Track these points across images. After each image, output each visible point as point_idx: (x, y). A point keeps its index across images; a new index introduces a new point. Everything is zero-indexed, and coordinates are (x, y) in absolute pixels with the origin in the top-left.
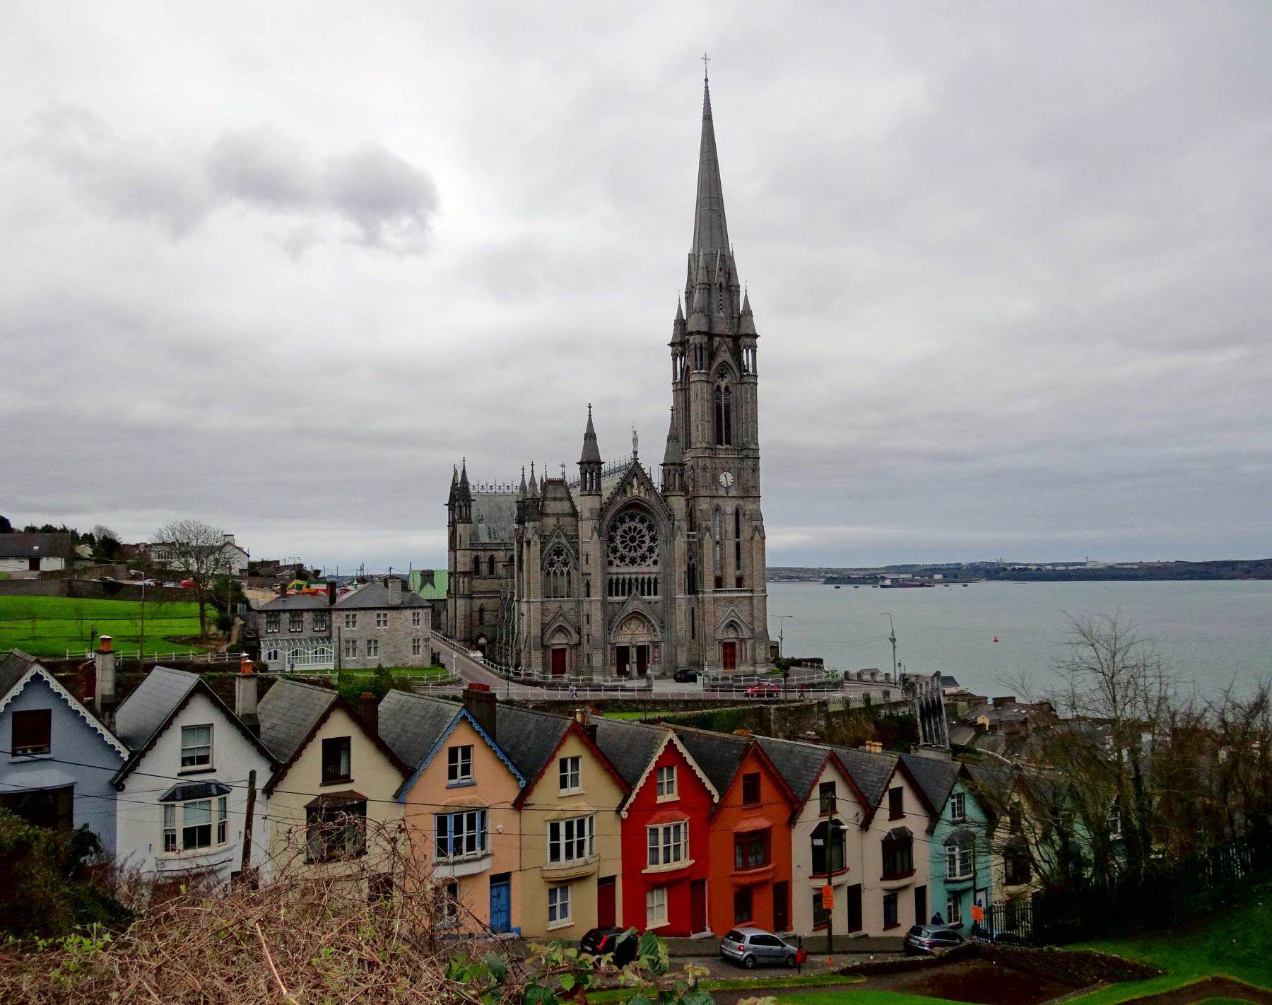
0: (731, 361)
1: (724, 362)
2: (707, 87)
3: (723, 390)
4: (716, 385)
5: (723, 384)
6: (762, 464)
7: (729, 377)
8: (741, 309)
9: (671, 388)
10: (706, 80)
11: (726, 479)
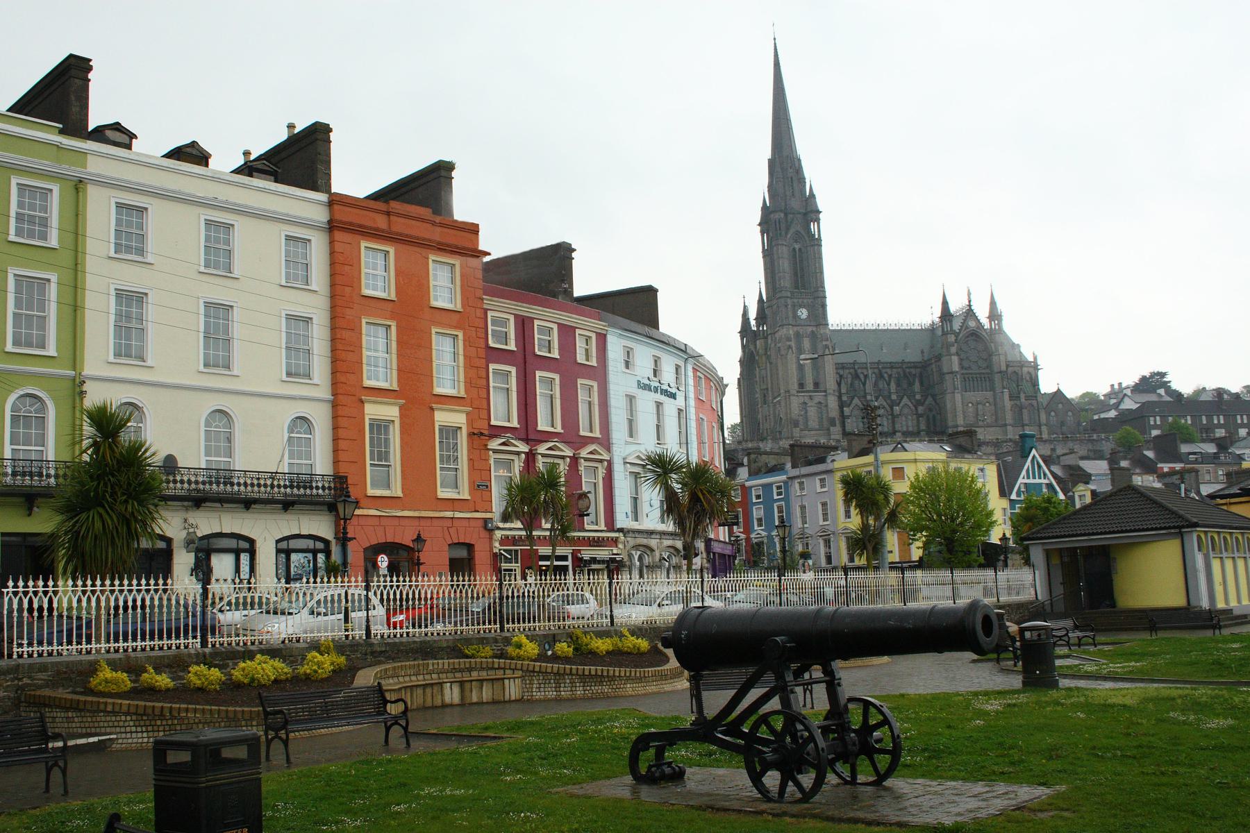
2: (775, 44)
5: (797, 246)
6: (829, 302)
8: (808, 194)
9: (761, 255)
10: (775, 39)
11: (803, 313)
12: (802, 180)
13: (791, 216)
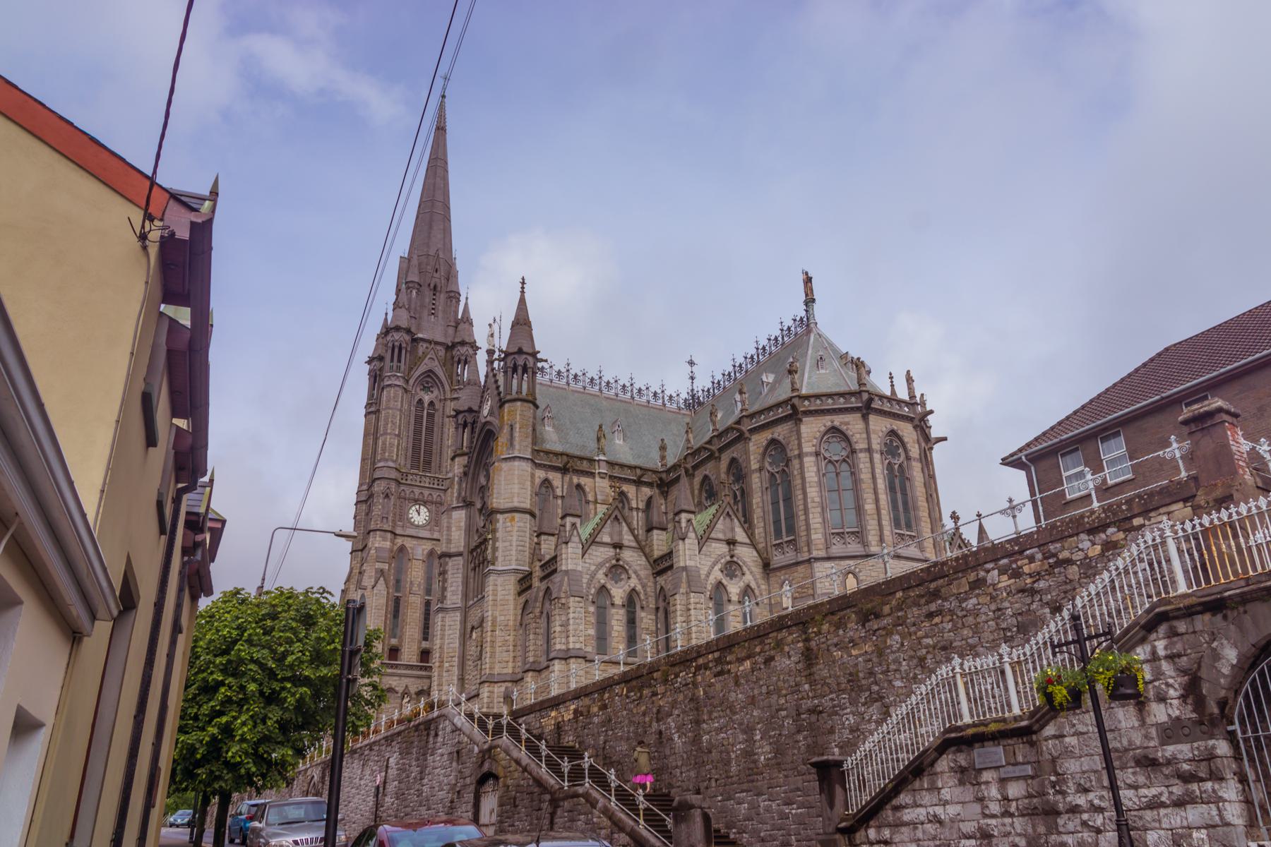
0: (440, 372)
1: (430, 371)
3: (426, 405)
4: (417, 399)
5: (427, 398)
7: (436, 392)
12: (454, 296)
13: (425, 345)
